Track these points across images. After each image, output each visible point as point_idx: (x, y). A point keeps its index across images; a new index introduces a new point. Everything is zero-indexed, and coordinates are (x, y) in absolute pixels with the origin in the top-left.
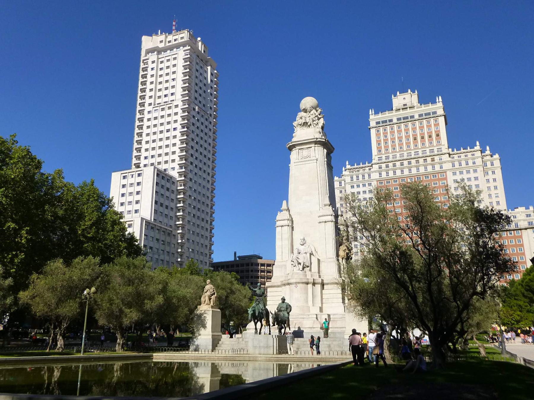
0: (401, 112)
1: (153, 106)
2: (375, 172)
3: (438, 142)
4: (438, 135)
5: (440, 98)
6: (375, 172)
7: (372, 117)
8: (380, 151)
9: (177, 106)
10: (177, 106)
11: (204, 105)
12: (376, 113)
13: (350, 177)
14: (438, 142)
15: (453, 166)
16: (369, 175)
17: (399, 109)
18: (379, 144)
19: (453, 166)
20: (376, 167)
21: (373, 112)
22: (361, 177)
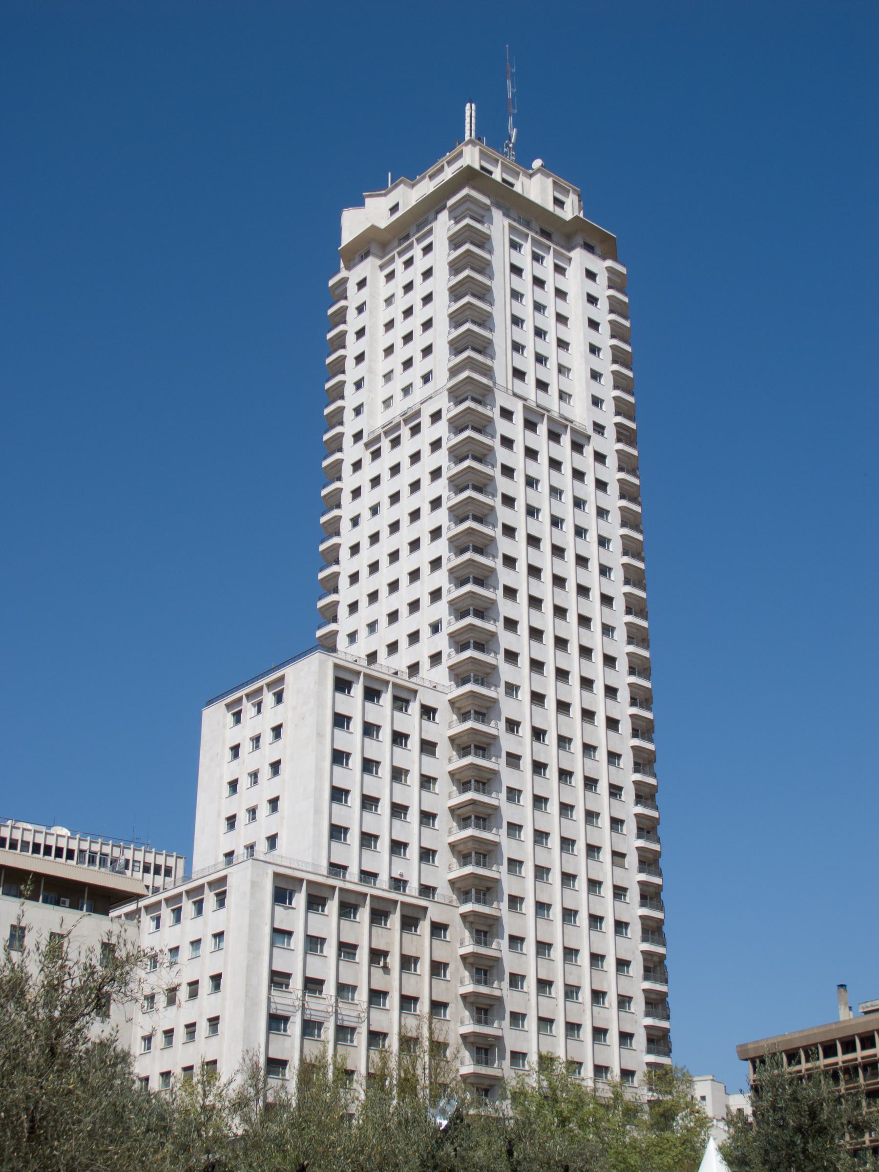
9: (436, 417)
10: (436, 417)
11: (563, 396)
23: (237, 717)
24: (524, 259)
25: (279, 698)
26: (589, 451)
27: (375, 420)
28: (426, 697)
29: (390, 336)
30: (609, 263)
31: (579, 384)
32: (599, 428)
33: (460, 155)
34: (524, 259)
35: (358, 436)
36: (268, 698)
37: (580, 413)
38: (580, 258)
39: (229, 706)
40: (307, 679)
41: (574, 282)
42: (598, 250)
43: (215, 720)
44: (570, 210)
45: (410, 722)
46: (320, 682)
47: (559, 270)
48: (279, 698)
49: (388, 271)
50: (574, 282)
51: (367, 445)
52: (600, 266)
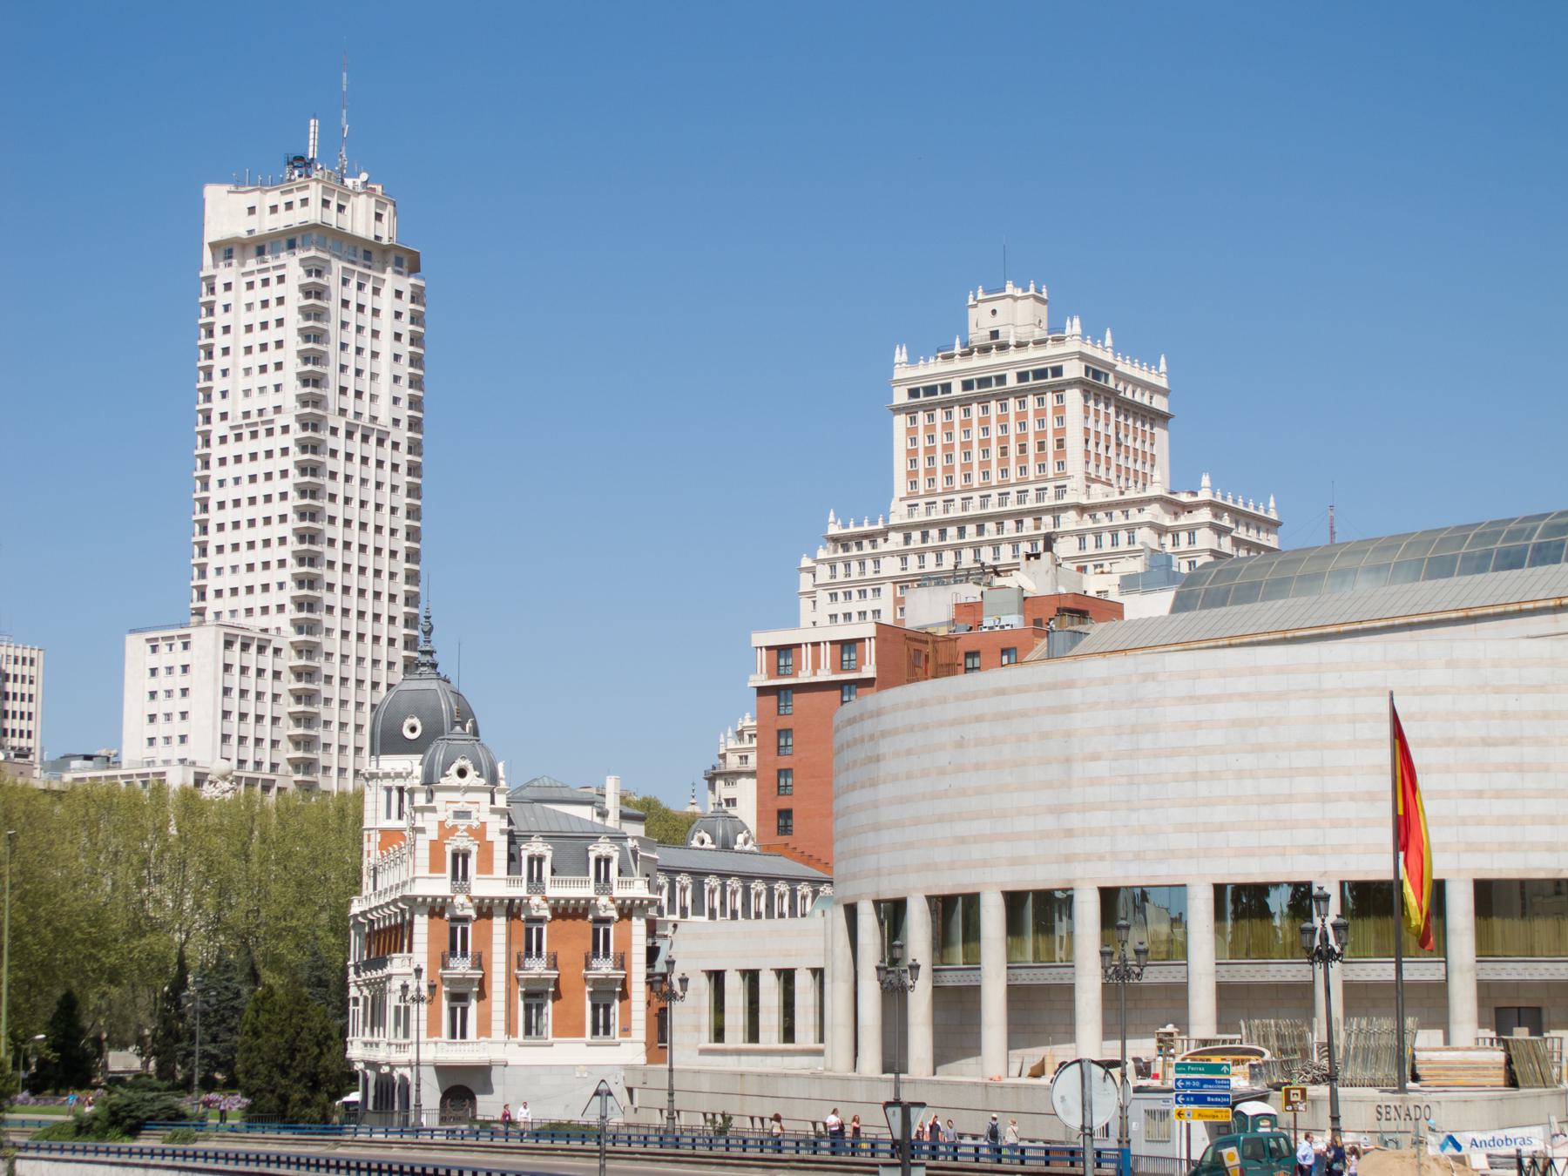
0: (977, 361)
1: (229, 422)
2: (891, 553)
3: (1061, 464)
4: (1060, 444)
5: (1077, 321)
6: (891, 553)
7: (899, 373)
8: (914, 484)
10: (285, 429)
12: (912, 361)
13: (827, 567)
14: (1061, 464)
15: (1082, 547)
16: (877, 562)
17: (971, 352)
18: (913, 462)
19: (1082, 547)
20: (896, 539)
21: (904, 357)
22: (855, 566)
23: (154, 649)
24: (351, 293)
25: (186, 646)
26: (388, 444)
27: (236, 405)
28: (276, 643)
29: (251, 334)
30: (412, 280)
31: (384, 388)
32: (396, 422)
33: (307, 187)
34: (351, 293)
35: (224, 416)
36: (178, 644)
37: (385, 412)
38: (391, 280)
39: (148, 640)
40: (206, 639)
41: (386, 302)
42: (406, 264)
43: (135, 646)
44: (386, 231)
45: (267, 661)
46: (216, 646)
47: (376, 291)
48: (186, 646)
49: (249, 279)
50: (386, 302)
51: (232, 428)
52: (407, 284)
